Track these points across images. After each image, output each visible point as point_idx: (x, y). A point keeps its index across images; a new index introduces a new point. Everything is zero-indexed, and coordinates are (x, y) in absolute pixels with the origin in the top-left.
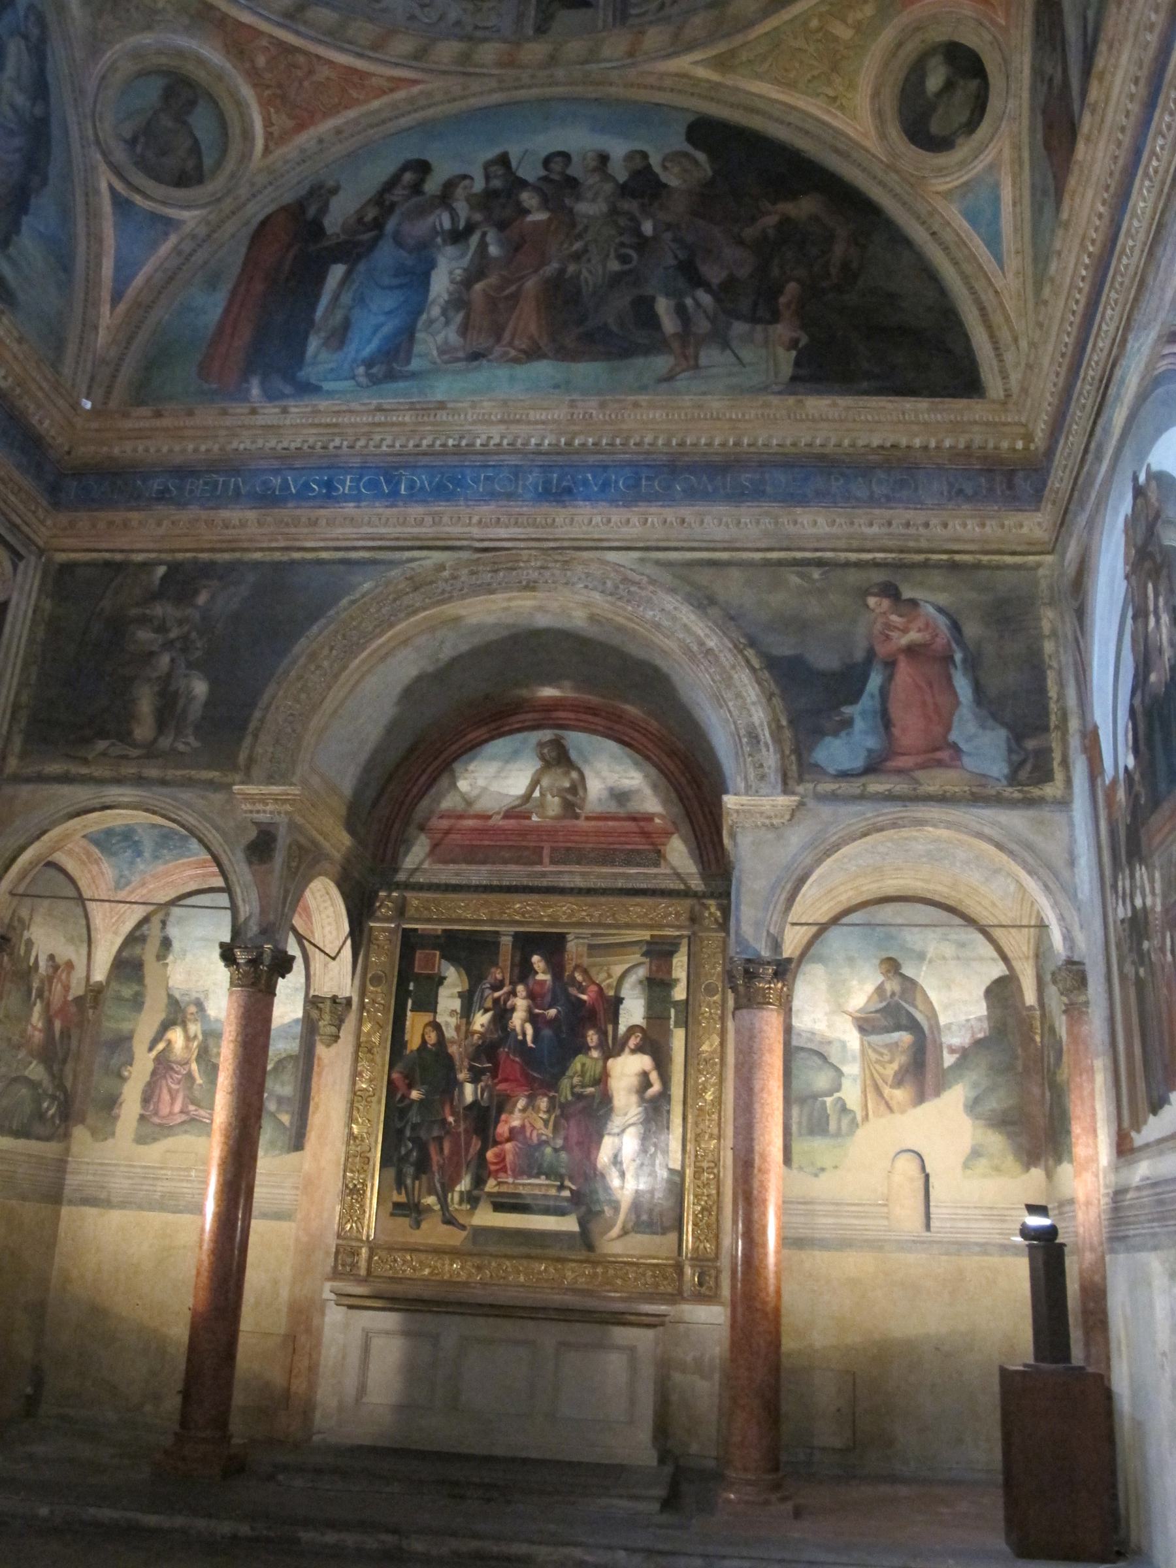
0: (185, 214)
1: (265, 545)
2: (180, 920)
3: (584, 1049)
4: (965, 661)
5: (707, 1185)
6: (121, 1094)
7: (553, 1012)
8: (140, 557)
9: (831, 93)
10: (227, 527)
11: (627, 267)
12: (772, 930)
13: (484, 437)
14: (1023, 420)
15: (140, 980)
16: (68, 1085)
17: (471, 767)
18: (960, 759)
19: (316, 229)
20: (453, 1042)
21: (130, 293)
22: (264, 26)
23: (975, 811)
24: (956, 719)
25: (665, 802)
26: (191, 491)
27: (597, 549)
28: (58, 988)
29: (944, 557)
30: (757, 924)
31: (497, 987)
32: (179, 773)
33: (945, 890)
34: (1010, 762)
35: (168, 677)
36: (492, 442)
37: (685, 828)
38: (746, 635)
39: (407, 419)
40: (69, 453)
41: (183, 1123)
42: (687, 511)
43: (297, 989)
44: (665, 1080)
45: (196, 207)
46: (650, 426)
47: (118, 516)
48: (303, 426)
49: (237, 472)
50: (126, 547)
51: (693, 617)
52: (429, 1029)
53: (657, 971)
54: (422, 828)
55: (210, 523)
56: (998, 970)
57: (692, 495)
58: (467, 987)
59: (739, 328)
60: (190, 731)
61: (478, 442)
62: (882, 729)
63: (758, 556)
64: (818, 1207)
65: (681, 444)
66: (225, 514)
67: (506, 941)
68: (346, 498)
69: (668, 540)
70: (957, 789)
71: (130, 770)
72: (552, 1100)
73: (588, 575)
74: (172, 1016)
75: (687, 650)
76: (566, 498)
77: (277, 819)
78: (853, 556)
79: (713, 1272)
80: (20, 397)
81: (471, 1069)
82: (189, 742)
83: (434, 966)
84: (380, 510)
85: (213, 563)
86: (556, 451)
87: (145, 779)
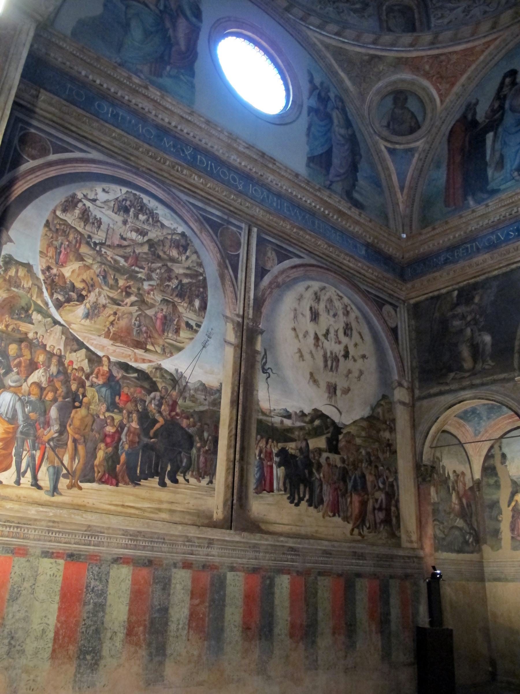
0: (418, 144)
1: (497, 267)
8: (444, 291)
10: (478, 265)
15: (496, 475)
16: (475, 527)
19: (474, 123)
21: (407, 183)
22: (423, 53)
26: (458, 256)
28: (460, 485)
32: (488, 378)
35: (472, 338)
40: (403, 258)
45: (421, 139)
47: (430, 276)
48: (497, 209)
49: (474, 240)
50: (438, 288)
55: (470, 266)
60: (488, 359)
66: (475, 260)
71: (467, 383)
74: (515, 489)
80: (378, 243)
85: (477, 283)
87: (474, 385)
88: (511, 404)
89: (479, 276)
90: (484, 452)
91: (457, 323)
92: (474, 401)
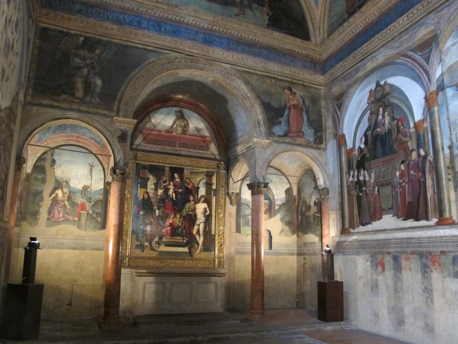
1: (119, 38)
2: (59, 154)
3: (189, 201)
4: (305, 111)
5: (221, 239)
6: (39, 211)
7: (180, 190)
8: (74, 32)
10: (106, 29)
13: (188, 19)
14: (320, 51)
15: (44, 173)
17: (155, 116)
18: (304, 135)
20: (152, 198)
23: (307, 149)
24: (303, 125)
25: (210, 133)
26: (91, 13)
27: (219, 62)
30: (260, 173)
31: (165, 182)
33: (277, 165)
34: (314, 138)
36: (190, 22)
37: (215, 141)
38: (257, 95)
39: (165, 7)
41: (63, 221)
42: (245, 56)
43: (101, 179)
44: (211, 210)
47: (66, 16)
50: (69, 27)
51: (245, 87)
52: (145, 194)
53: (209, 180)
54: (140, 132)
56: (288, 186)
57: (243, 52)
58: (156, 182)
59: (255, 5)
60: (96, 96)
61: (186, 20)
63: (260, 73)
64: (247, 244)
65: (241, 36)
67: (167, 169)
68: (146, 29)
69: (238, 63)
70: (304, 143)
72: (181, 215)
74: (57, 186)
75: (243, 96)
76: (210, 44)
77: (127, 129)
78: (282, 78)
79: (222, 261)
81: (158, 206)
82: (96, 100)
83: (146, 174)
84: (158, 36)
86: (207, 29)
87: (81, 110)
88: (105, 133)
89: (104, 37)
90: (39, 155)
91: (77, 61)
92: (77, 121)
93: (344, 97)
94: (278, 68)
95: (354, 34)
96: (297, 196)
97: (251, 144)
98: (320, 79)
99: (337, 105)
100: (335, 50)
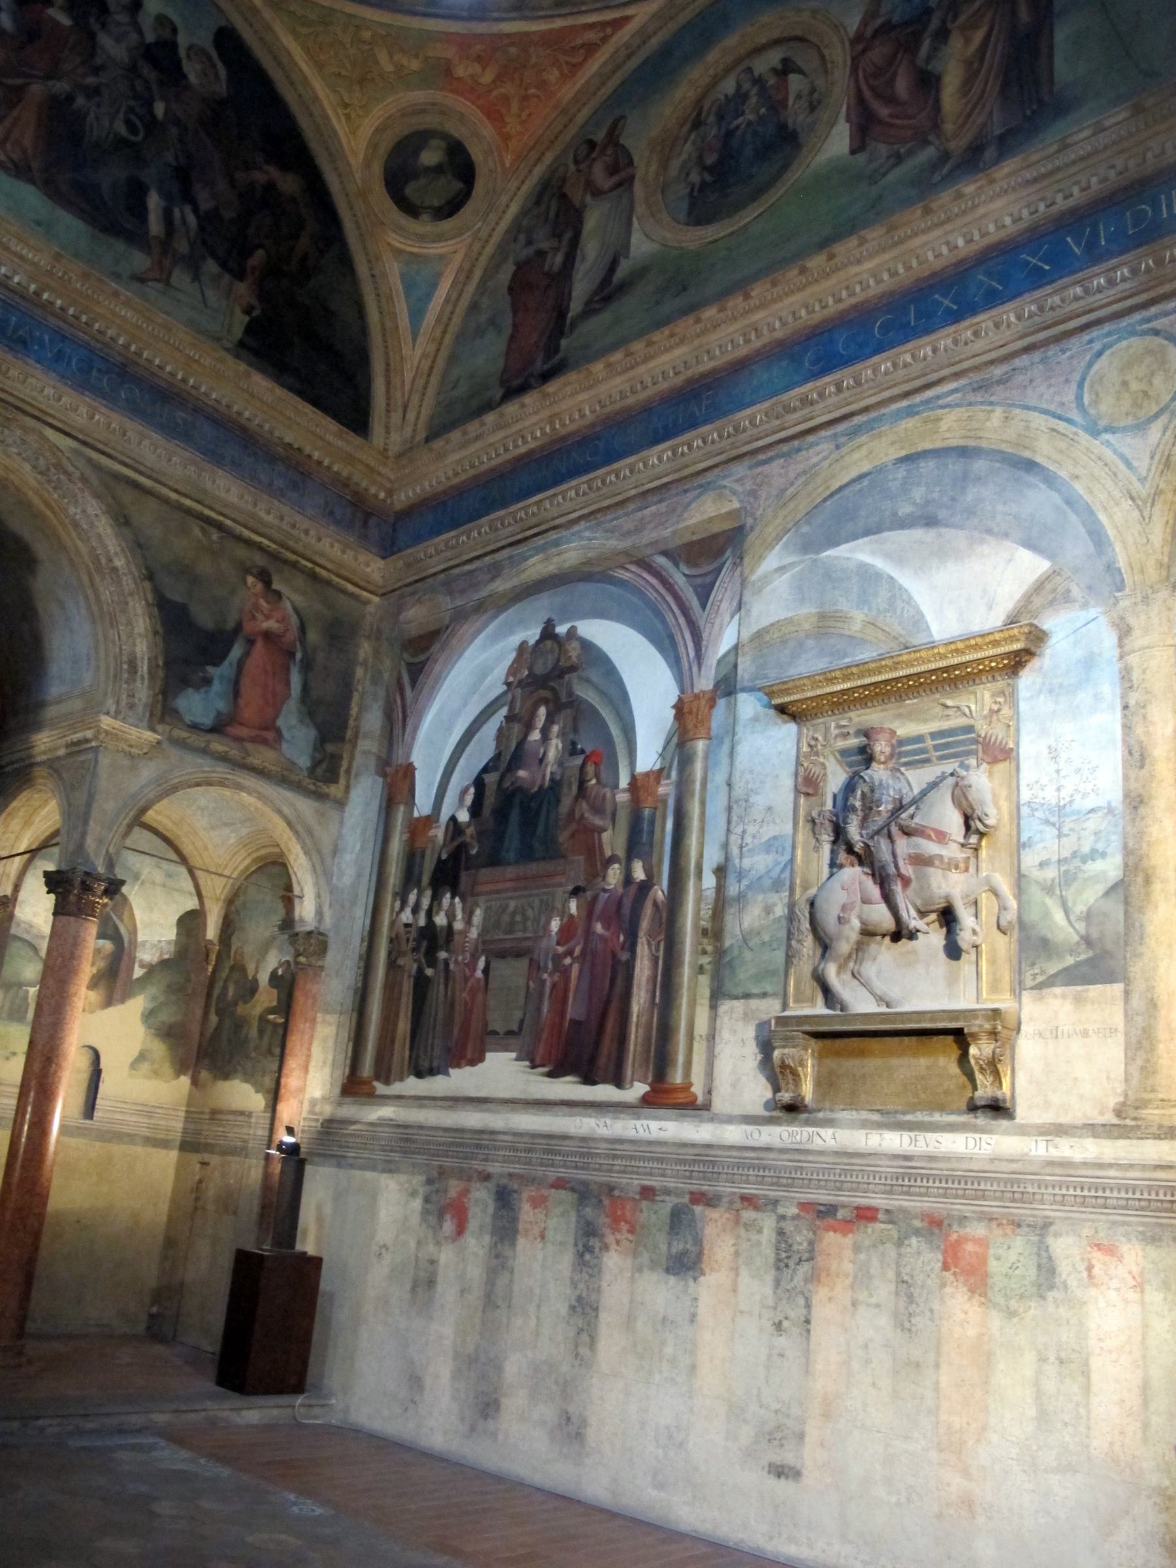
4: (302, 661)
9: (347, 101)
11: (133, 138)
12: (111, 850)
14: (392, 477)
23: (280, 790)
24: (285, 708)
27: (38, 419)
29: (310, 565)
30: (100, 842)
33: (170, 825)
34: (313, 758)
38: (147, 568)
42: (134, 427)
46: (118, 321)
51: (109, 531)
56: (192, 904)
57: (134, 410)
59: (211, 266)
62: (231, 696)
63: (173, 496)
70: (273, 768)
73: (24, 442)
75: (96, 559)
78: (246, 533)
93: (436, 647)
94: (241, 497)
95: (508, 456)
96: (216, 942)
97: (89, 734)
98: (374, 568)
99: (410, 665)
100: (440, 489)
